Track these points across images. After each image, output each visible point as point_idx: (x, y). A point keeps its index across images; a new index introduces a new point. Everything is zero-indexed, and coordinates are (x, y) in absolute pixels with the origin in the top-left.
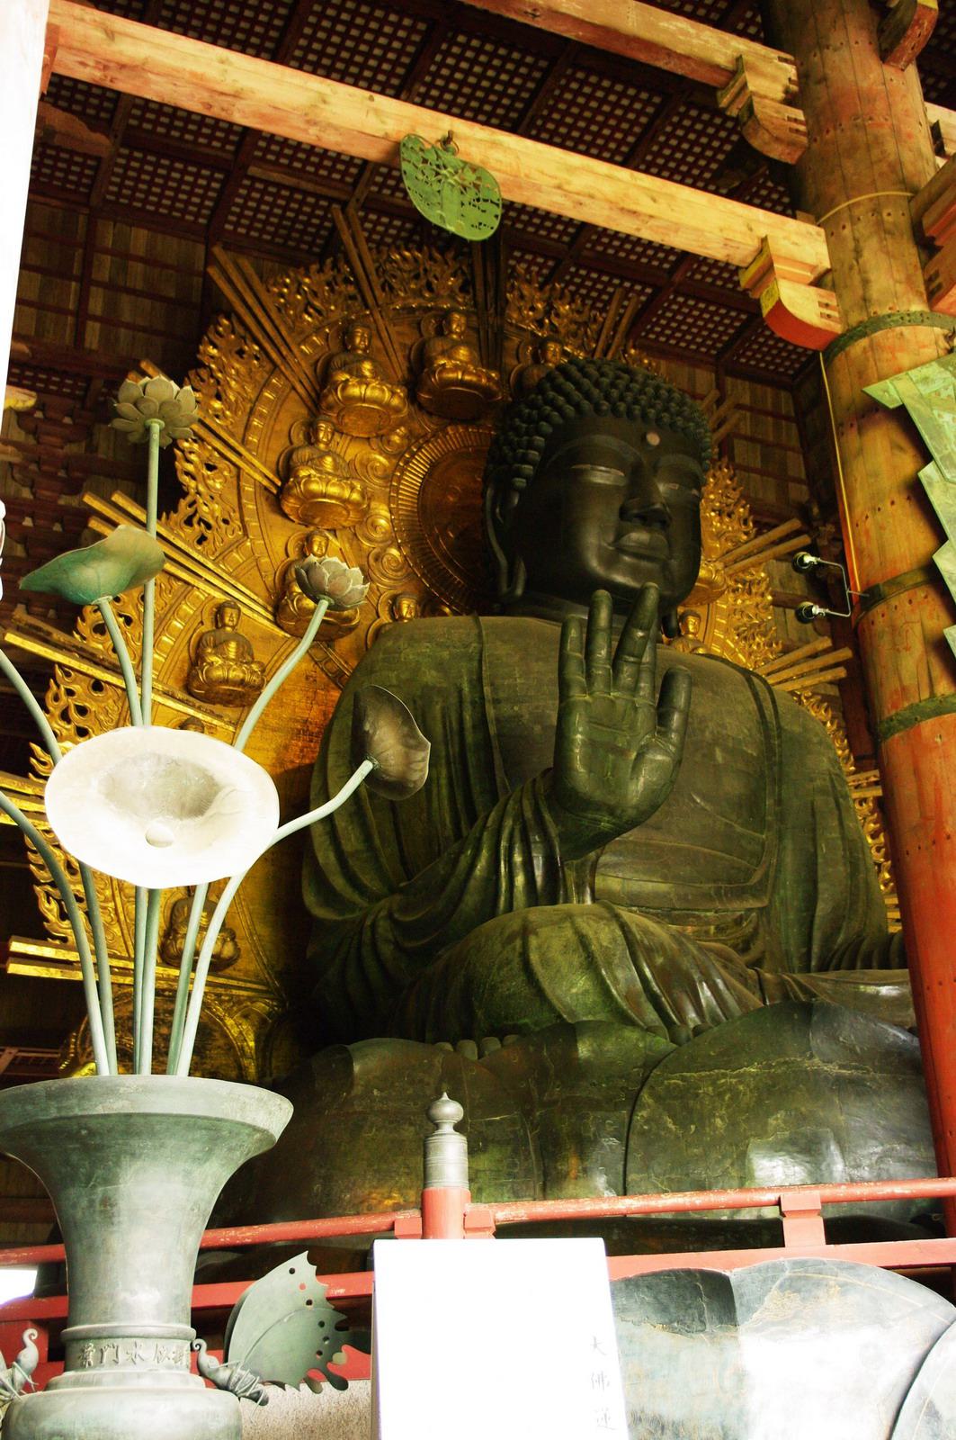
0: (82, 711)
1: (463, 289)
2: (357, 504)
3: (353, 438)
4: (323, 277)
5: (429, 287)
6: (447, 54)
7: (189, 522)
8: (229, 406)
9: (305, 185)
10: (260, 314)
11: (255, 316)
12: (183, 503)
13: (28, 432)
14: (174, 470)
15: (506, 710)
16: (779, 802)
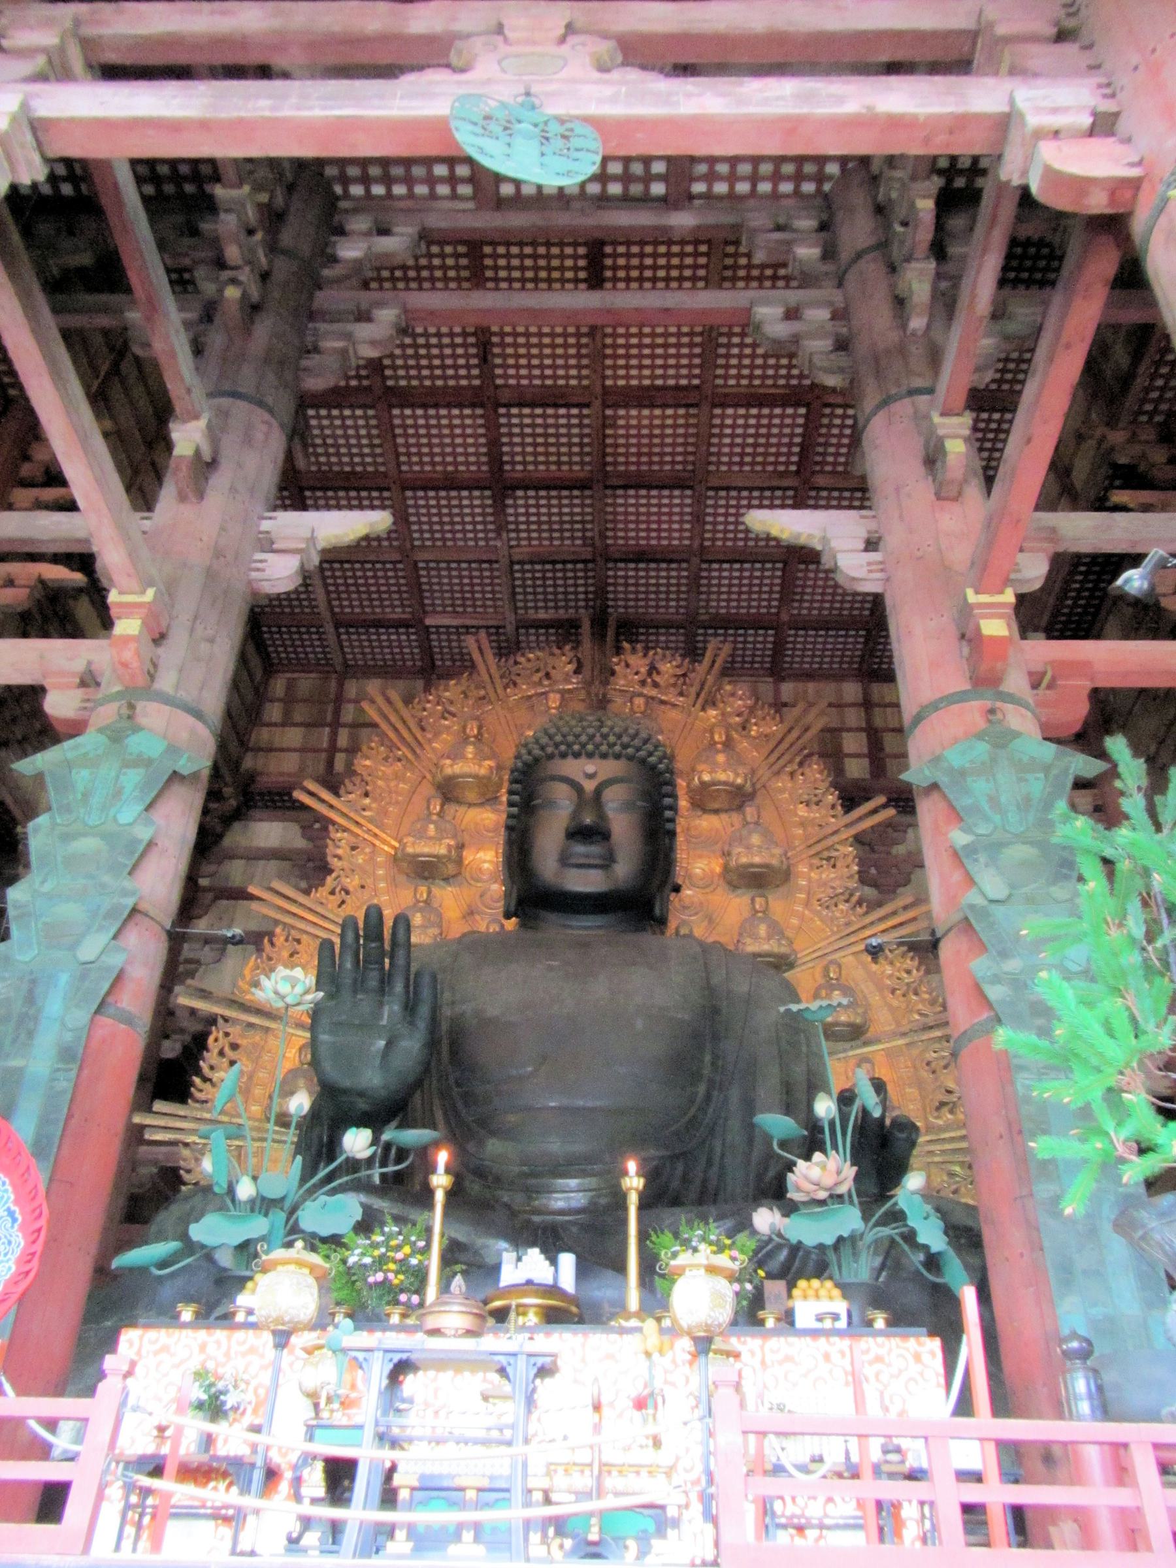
0: (235, 1047)
1: (577, 672)
2: (448, 858)
3: (470, 805)
4: (460, 689)
5: (548, 676)
6: (516, 506)
7: (332, 893)
8: (374, 800)
9: (469, 622)
10: (399, 726)
11: (396, 730)
12: (329, 880)
13: (310, 839)
14: (324, 855)
15: (458, 1009)
16: (716, 1057)
